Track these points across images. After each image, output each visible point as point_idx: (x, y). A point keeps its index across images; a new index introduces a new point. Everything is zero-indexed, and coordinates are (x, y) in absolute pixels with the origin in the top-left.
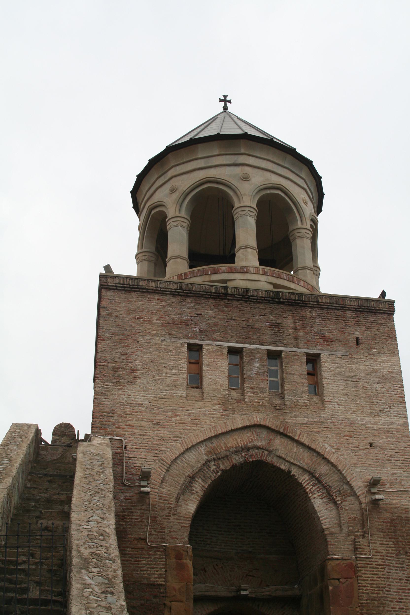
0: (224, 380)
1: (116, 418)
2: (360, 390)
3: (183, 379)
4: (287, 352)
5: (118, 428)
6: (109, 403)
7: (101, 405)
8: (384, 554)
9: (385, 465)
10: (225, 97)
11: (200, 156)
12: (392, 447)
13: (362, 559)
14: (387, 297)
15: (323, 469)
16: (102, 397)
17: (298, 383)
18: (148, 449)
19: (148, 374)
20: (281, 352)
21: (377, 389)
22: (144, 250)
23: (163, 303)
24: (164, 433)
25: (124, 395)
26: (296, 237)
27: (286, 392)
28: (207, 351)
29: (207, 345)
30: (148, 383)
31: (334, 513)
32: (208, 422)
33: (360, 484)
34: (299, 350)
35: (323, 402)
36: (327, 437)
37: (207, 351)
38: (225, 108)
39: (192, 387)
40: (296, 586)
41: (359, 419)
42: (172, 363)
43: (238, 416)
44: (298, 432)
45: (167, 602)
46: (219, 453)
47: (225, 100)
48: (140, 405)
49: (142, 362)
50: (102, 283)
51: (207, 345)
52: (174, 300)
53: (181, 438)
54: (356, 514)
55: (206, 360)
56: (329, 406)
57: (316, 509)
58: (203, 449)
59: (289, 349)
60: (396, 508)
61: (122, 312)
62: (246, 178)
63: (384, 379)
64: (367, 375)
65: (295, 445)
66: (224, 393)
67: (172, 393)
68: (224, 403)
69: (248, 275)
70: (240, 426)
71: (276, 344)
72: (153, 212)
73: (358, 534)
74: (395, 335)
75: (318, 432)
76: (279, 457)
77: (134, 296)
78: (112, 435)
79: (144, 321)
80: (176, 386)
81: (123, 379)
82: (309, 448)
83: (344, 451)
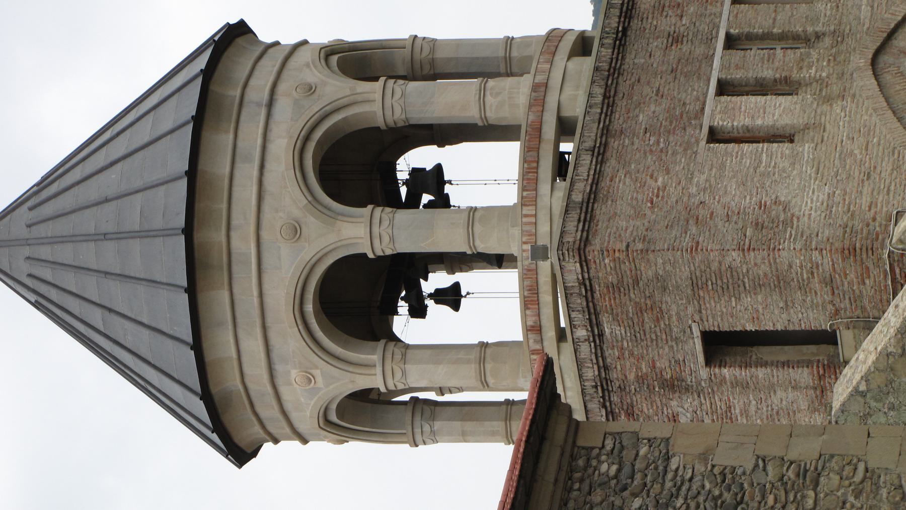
1: (856, 223)
4: (729, 26)
5: (874, 219)
6: (827, 232)
7: (831, 241)
16: (815, 239)
17: (792, 15)
19: (768, 189)
25: (810, 215)
26: (431, 56)
42: (748, 161)
49: (745, 197)
67: (807, 160)
69: (551, 83)
70: (873, 81)
72: (309, 308)
79: (658, 196)
81: (778, 217)
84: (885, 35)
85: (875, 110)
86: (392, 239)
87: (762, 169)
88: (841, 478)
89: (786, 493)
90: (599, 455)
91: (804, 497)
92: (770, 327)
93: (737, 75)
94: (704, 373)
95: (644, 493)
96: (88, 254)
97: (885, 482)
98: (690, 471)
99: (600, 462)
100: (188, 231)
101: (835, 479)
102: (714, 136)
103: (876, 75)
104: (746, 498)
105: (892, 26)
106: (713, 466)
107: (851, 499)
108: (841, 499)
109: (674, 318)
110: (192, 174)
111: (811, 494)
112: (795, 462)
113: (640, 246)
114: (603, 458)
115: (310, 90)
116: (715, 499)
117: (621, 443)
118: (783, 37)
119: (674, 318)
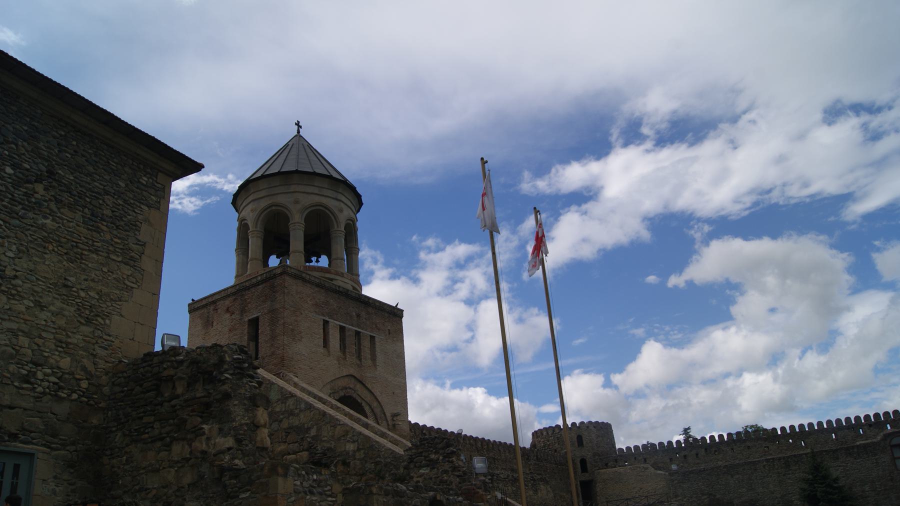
4: (363, 333)
5: (295, 368)
10: (298, 122)
11: (316, 185)
14: (398, 307)
15: (375, 404)
20: (360, 332)
22: (258, 229)
23: (312, 291)
33: (389, 415)
35: (375, 365)
38: (299, 132)
44: (367, 382)
47: (298, 124)
52: (316, 289)
56: (378, 367)
71: (358, 327)
72: (274, 208)
75: (374, 383)
76: (358, 395)
82: (371, 392)
84: (361, 380)
85: (335, 374)
86: (294, 229)
87: (314, 335)
88: (128, 276)
89: (121, 249)
90: (153, 180)
91: (118, 256)
92: (260, 337)
93: (347, 334)
94: (246, 319)
95: (127, 189)
97: (123, 294)
98: (139, 212)
99: (148, 178)
100: (297, 172)
101: (129, 273)
102: (326, 323)
103: (347, 376)
104: (119, 230)
105: (364, 383)
106: (141, 223)
107: (114, 276)
108: (115, 272)
109: (263, 306)
110: (315, 174)
111: (120, 259)
112: (140, 258)
113: (286, 291)
114: (151, 180)
115: (341, 211)
116: (121, 218)
117: (158, 190)
118: (360, 349)
119: (263, 306)
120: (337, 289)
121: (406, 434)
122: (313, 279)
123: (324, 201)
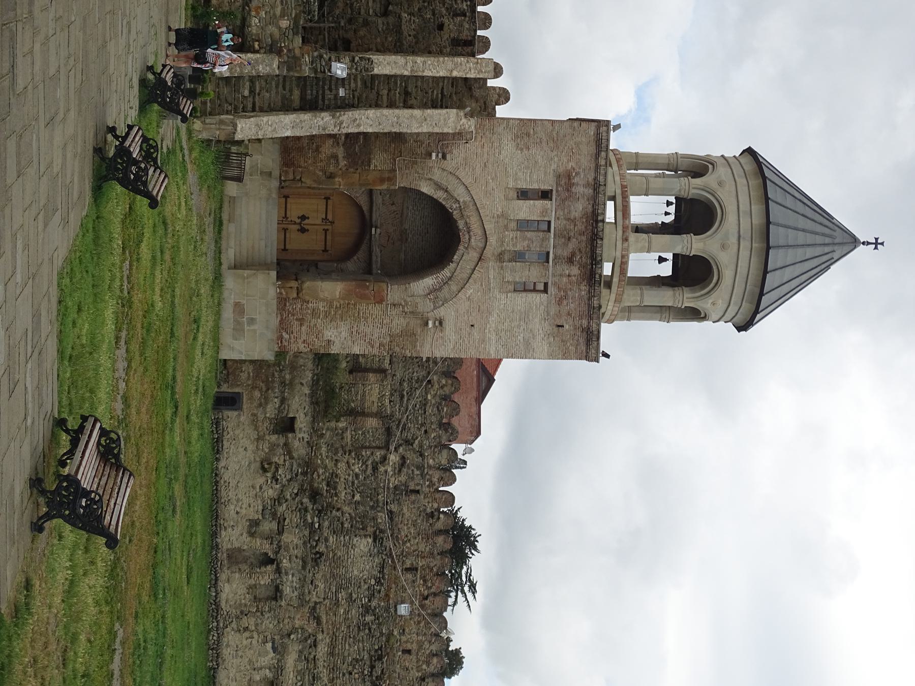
0: (522, 216)
2: (518, 323)
3: (523, 185)
4: (548, 267)
8: (390, 325)
9: (457, 335)
11: (753, 207)
12: (471, 342)
13: (387, 308)
14: (602, 359)
15: (454, 288)
18: (465, 159)
21: (519, 337)
22: (680, 160)
24: (478, 171)
27: (514, 263)
28: (546, 204)
29: (552, 204)
30: (518, 159)
31: (421, 293)
32: (488, 203)
34: (550, 277)
36: (478, 292)
37: (546, 204)
38: (863, 243)
39: (518, 193)
40: (379, 272)
41: (493, 319)
43: (493, 226)
44: (482, 271)
45: (358, 171)
46: (465, 211)
48: (500, 153)
50: (601, 123)
51: (552, 204)
53: (475, 182)
54: (420, 309)
55: (540, 203)
57: (425, 280)
58: (468, 199)
59: (551, 269)
60: (424, 339)
61: (577, 139)
62: (723, 247)
63: (527, 343)
64: (531, 330)
65: (472, 267)
66: (511, 216)
68: (503, 215)
69: (621, 242)
73: (406, 309)
74: (566, 358)
77: (593, 149)
78: (476, 133)
80: (516, 179)
83: (468, 303)
96: (810, 238)
115: (723, 247)
120: (600, 218)
121: (418, 348)
122: (602, 172)
123: (731, 218)
